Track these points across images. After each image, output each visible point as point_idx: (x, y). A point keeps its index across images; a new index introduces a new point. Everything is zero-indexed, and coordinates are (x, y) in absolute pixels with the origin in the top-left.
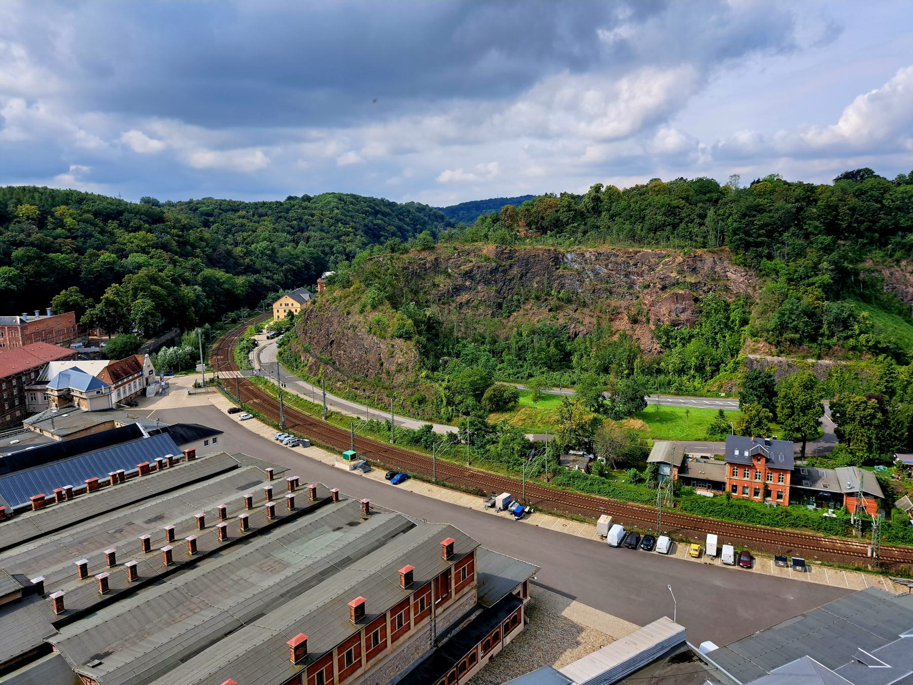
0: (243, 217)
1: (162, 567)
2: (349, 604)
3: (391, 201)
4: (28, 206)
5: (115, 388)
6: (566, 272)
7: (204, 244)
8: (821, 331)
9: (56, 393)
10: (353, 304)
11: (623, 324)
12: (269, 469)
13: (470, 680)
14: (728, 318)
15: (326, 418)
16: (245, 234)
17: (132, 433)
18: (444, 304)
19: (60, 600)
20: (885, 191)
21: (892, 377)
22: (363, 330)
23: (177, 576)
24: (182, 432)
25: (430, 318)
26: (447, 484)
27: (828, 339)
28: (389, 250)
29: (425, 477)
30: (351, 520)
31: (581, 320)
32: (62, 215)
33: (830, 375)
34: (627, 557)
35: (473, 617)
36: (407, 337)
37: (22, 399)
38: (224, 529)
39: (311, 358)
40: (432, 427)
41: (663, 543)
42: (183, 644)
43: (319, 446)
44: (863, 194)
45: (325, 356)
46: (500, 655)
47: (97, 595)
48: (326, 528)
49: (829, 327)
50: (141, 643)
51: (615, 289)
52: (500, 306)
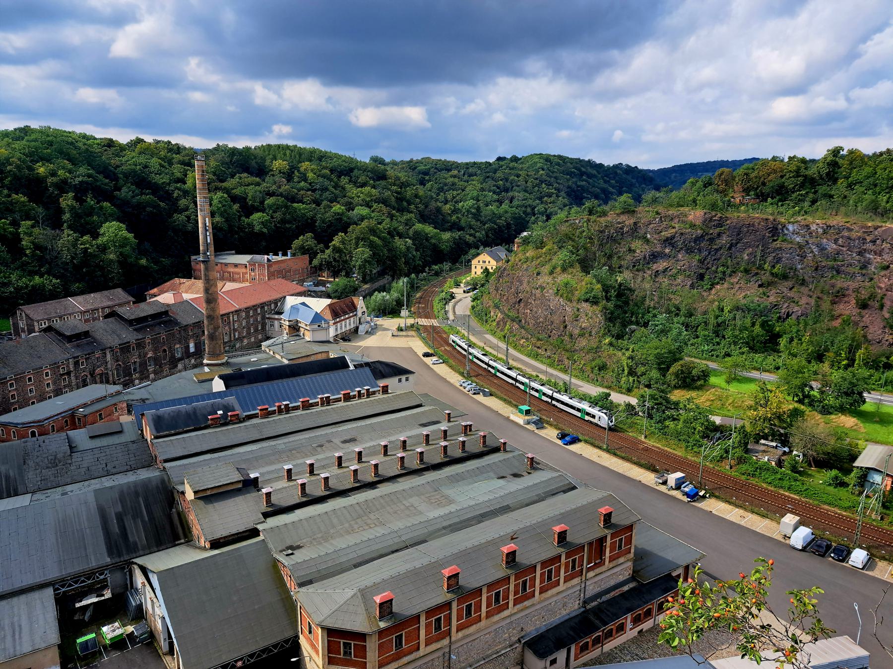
0: (455, 177)
1: (349, 483)
2: (502, 549)
3: (598, 162)
4: (280, 161)
6: (785, 245)
9: (287, 323)
11: (848, 309)
12: (447, 412)
13: (615, 648)
16: (455, 193)
17: (341, 364)
18: (638, 270)
19: (268, 495)
24: (381, 368)
25: (620, 285)
26: (619, 453)
28: (586, 213)
29: (597, 443)
30: (515, 471)
31: (796, 299)
32: (305, 170)
34: (812, 563)
35: (626, 588)
36: (594, 302)
37: (264, 325)
38: (402, 458)
39: (499, 314)
41: (858, 556)
45: (513, 314)
46: (650, 631)
47: (296, 497)
48: (492, 474)
51: (843, 268)
52: (701, 277)
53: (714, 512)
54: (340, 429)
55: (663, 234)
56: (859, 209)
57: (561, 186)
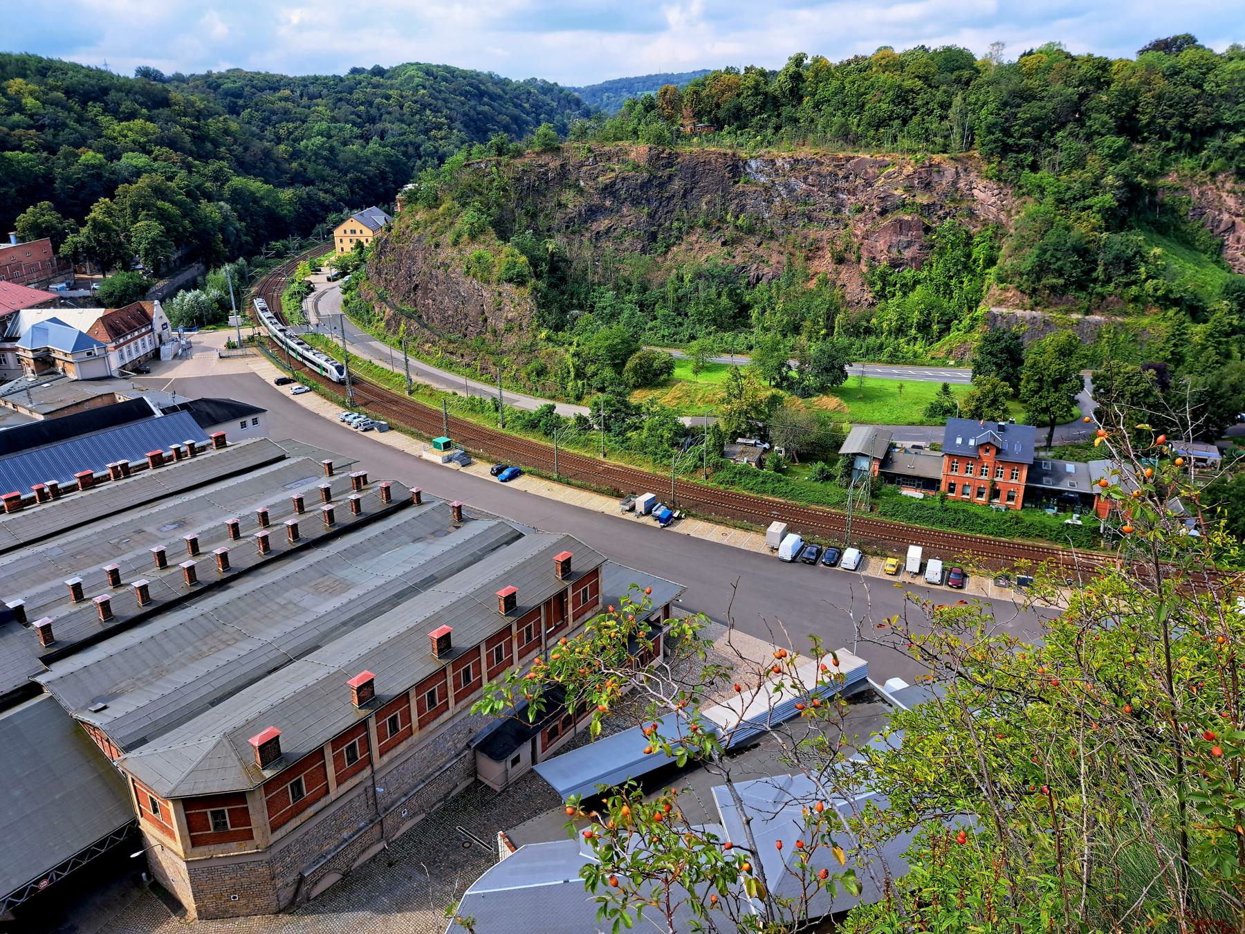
0: (286, 99)
1: (182, 587)
2: (431, 634)
5: (116, 348)
8: (1094, 275)
10: (443, 233)
11: (823, 265)
12: (326, 462)
14: (969, 256)
15: (411, 393)
16: (291, 125)
17: (138, 410)
18: (573, 233)
19: (46, 629)
20: (1209, 70)
21: (1182, 340)
23: (205, 598)
24: (209, 410)
25: (553, 255)
26: (574, 482)
28: (493, 152)
29: (544, 473)
31: (765, 258)
34: (804, 574)
36: (520, 281)
38: (265, 539)
39: (388, 309)
40: (554, 407)
41: (850, 556)
42: (213, 684)
44: (1177, 73)
45: (407, 308)
47: (97, 623)
49: (1105, 270)
50: (157, 683)
52: (653, 237)
53: (692, 535)
55: (600, 179)
56: (829, 135)
57: (454, 114)
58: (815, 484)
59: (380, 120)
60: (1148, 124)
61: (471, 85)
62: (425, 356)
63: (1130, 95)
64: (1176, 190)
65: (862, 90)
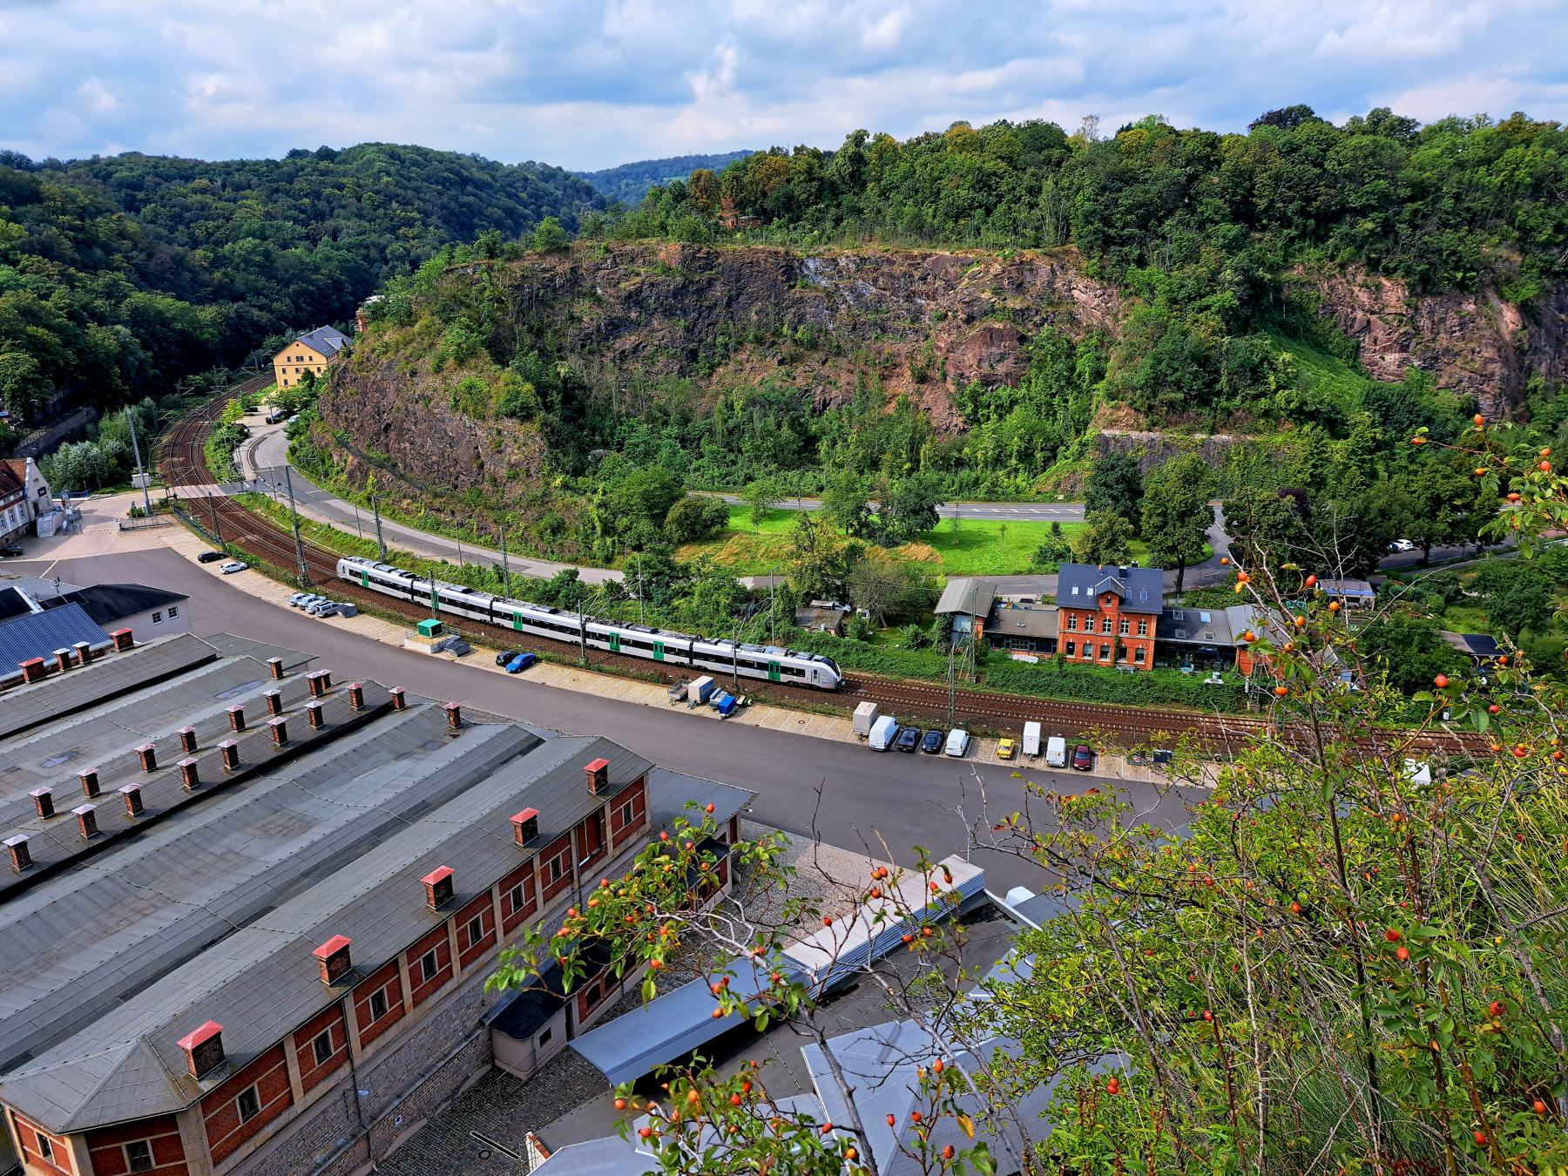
0: (203, 191)
1: (78, 842)
2: (425, 880)
7: (127, 244)
8: (1218, 387)
11: (903, 385)
12: (273, 660)
14: (1072, 369)
16: (211, 224)
18: (591, 352)
20: (1330, 146)
22: (443, 404)
23: (108, 855)
24: (107, 600)
25: (565, 381)
26: (606, 667)
27: (1227, 400)
28: (483, 253)
29: (567, 658)
31: (833, 379)
33: (1228, 459)
34: (899, 765)
36: (525, 415)
38: (191, 769)
39: (351, 457)
41: (956, 739)
42: (124, 970)
43: (374, 614)
44: (1294, 150)
45: (377, 454)
48: (384, 755)
49: (1230, 380)
52: (693, 356)
53: (762, 725)
54: (36, 738)
55: (622, 285)
56: (900, 228)
58: (908, 652)
59: (331, 216)
60: (1267, 209)
61: (450, 170)
62: (403, 515)
63: (1243, 176)
64: (1303, 285)
65: (936, 174)
